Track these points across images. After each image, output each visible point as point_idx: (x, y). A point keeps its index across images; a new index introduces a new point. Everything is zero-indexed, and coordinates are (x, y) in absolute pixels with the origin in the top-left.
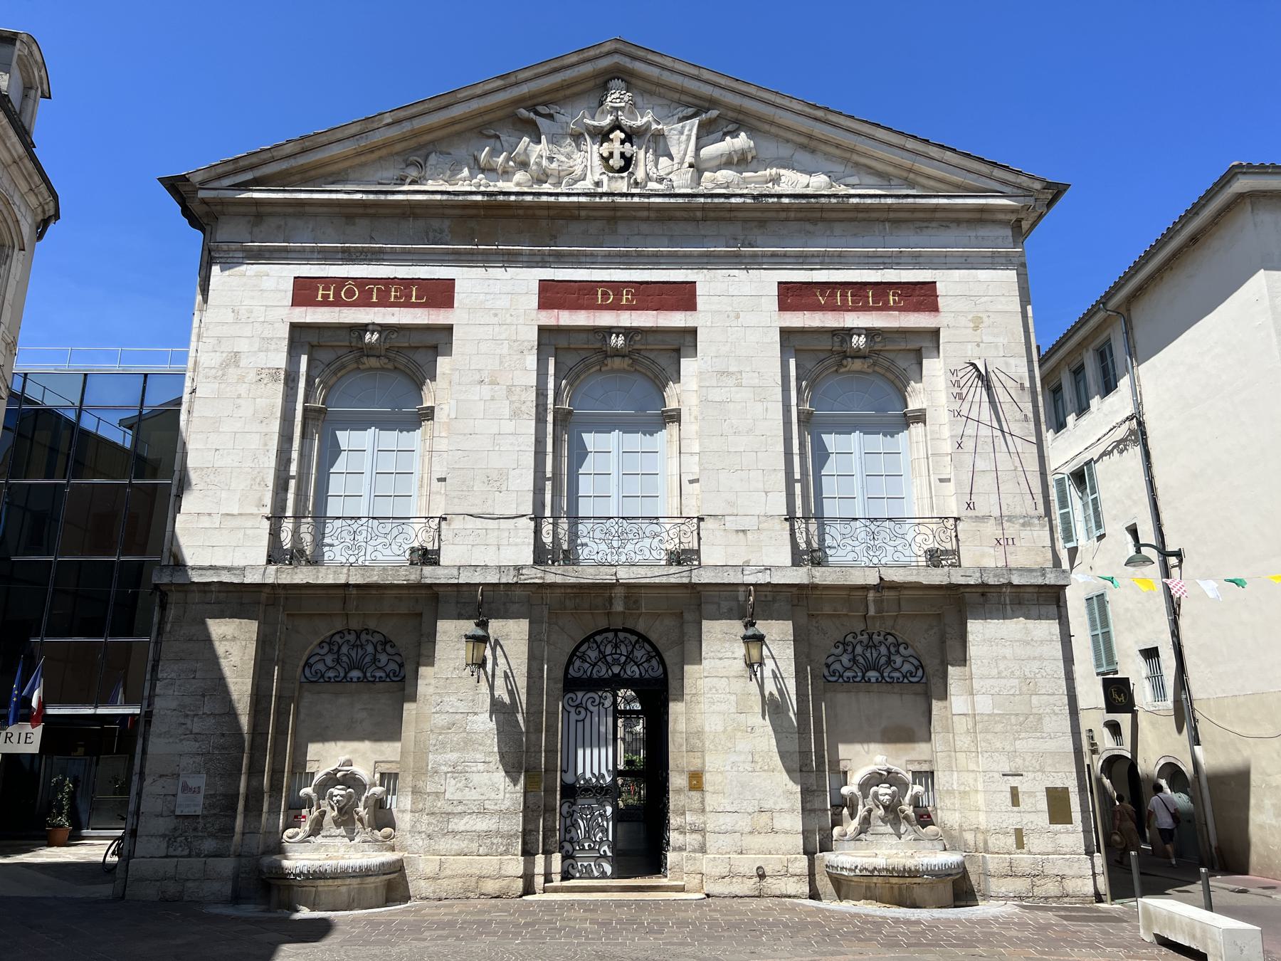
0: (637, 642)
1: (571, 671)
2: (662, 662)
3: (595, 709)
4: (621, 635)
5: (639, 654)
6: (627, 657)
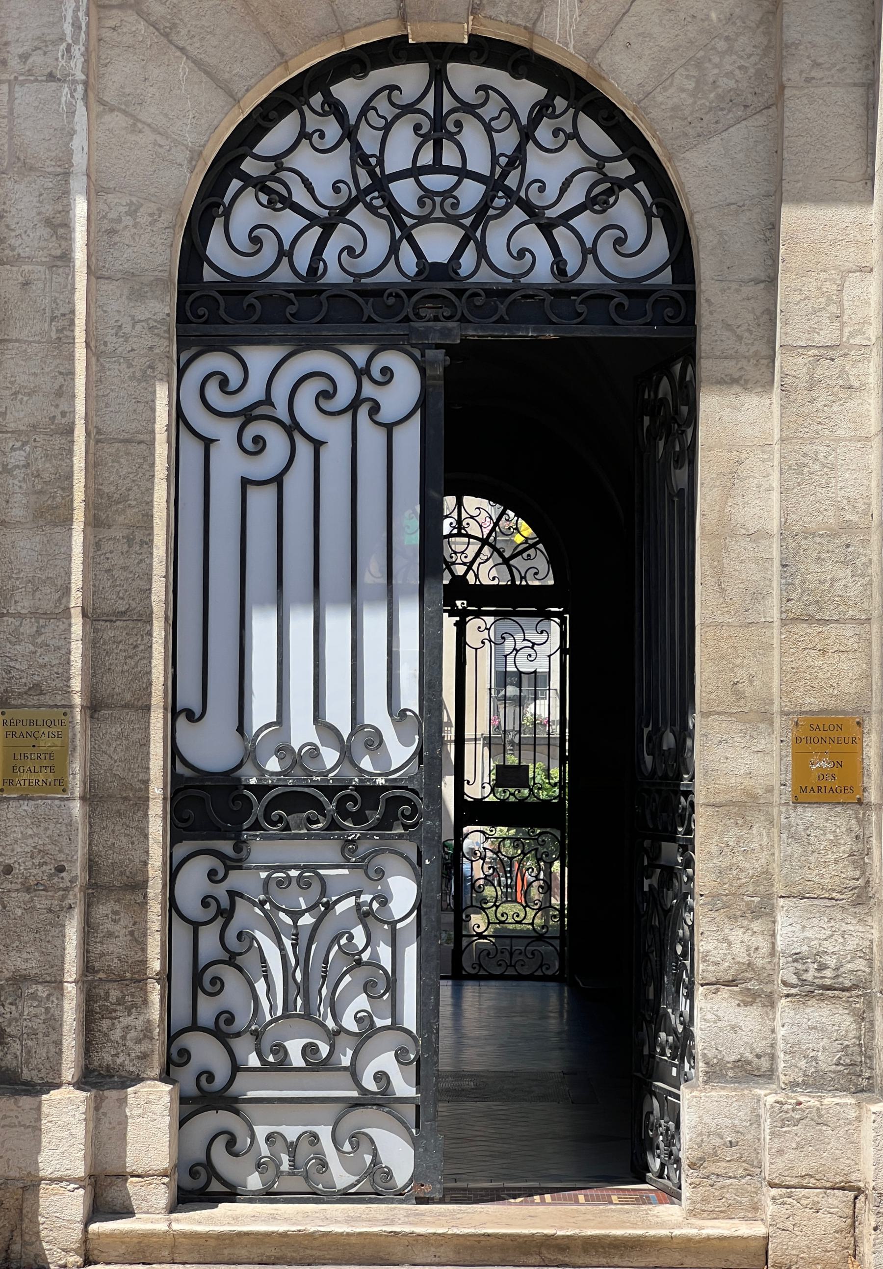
0: (542, 109)
1: (216, 247)
2: (667, 208)
3: (334, 432)
4: (464, 77)
5: (552, 169)
6: (494, 184)
